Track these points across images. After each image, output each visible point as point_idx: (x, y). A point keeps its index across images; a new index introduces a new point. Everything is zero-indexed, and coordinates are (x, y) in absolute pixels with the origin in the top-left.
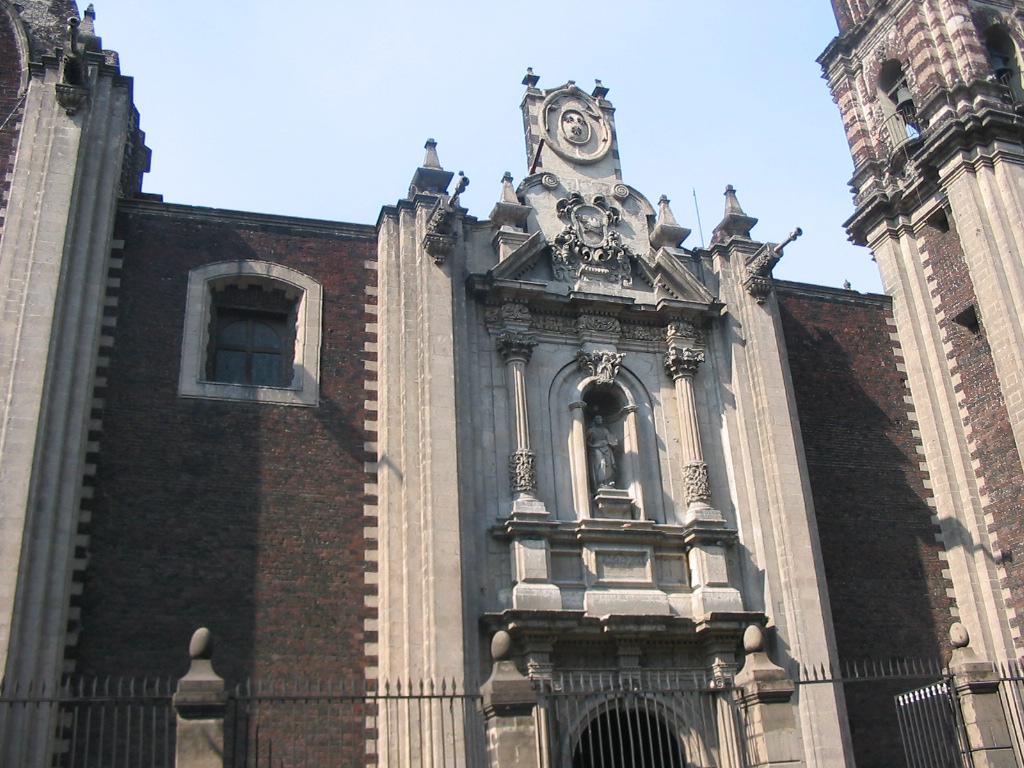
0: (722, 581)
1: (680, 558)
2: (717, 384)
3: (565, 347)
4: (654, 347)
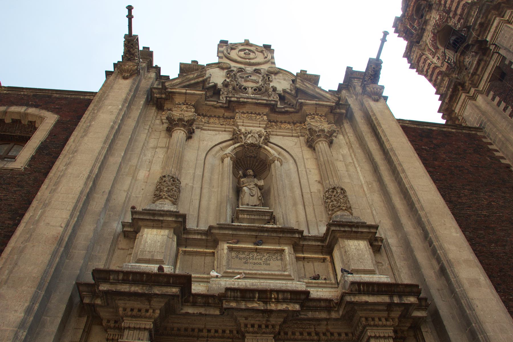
0: (367, 268)
1: (324, 260)
2: (351, 150)
4: (297, 133)
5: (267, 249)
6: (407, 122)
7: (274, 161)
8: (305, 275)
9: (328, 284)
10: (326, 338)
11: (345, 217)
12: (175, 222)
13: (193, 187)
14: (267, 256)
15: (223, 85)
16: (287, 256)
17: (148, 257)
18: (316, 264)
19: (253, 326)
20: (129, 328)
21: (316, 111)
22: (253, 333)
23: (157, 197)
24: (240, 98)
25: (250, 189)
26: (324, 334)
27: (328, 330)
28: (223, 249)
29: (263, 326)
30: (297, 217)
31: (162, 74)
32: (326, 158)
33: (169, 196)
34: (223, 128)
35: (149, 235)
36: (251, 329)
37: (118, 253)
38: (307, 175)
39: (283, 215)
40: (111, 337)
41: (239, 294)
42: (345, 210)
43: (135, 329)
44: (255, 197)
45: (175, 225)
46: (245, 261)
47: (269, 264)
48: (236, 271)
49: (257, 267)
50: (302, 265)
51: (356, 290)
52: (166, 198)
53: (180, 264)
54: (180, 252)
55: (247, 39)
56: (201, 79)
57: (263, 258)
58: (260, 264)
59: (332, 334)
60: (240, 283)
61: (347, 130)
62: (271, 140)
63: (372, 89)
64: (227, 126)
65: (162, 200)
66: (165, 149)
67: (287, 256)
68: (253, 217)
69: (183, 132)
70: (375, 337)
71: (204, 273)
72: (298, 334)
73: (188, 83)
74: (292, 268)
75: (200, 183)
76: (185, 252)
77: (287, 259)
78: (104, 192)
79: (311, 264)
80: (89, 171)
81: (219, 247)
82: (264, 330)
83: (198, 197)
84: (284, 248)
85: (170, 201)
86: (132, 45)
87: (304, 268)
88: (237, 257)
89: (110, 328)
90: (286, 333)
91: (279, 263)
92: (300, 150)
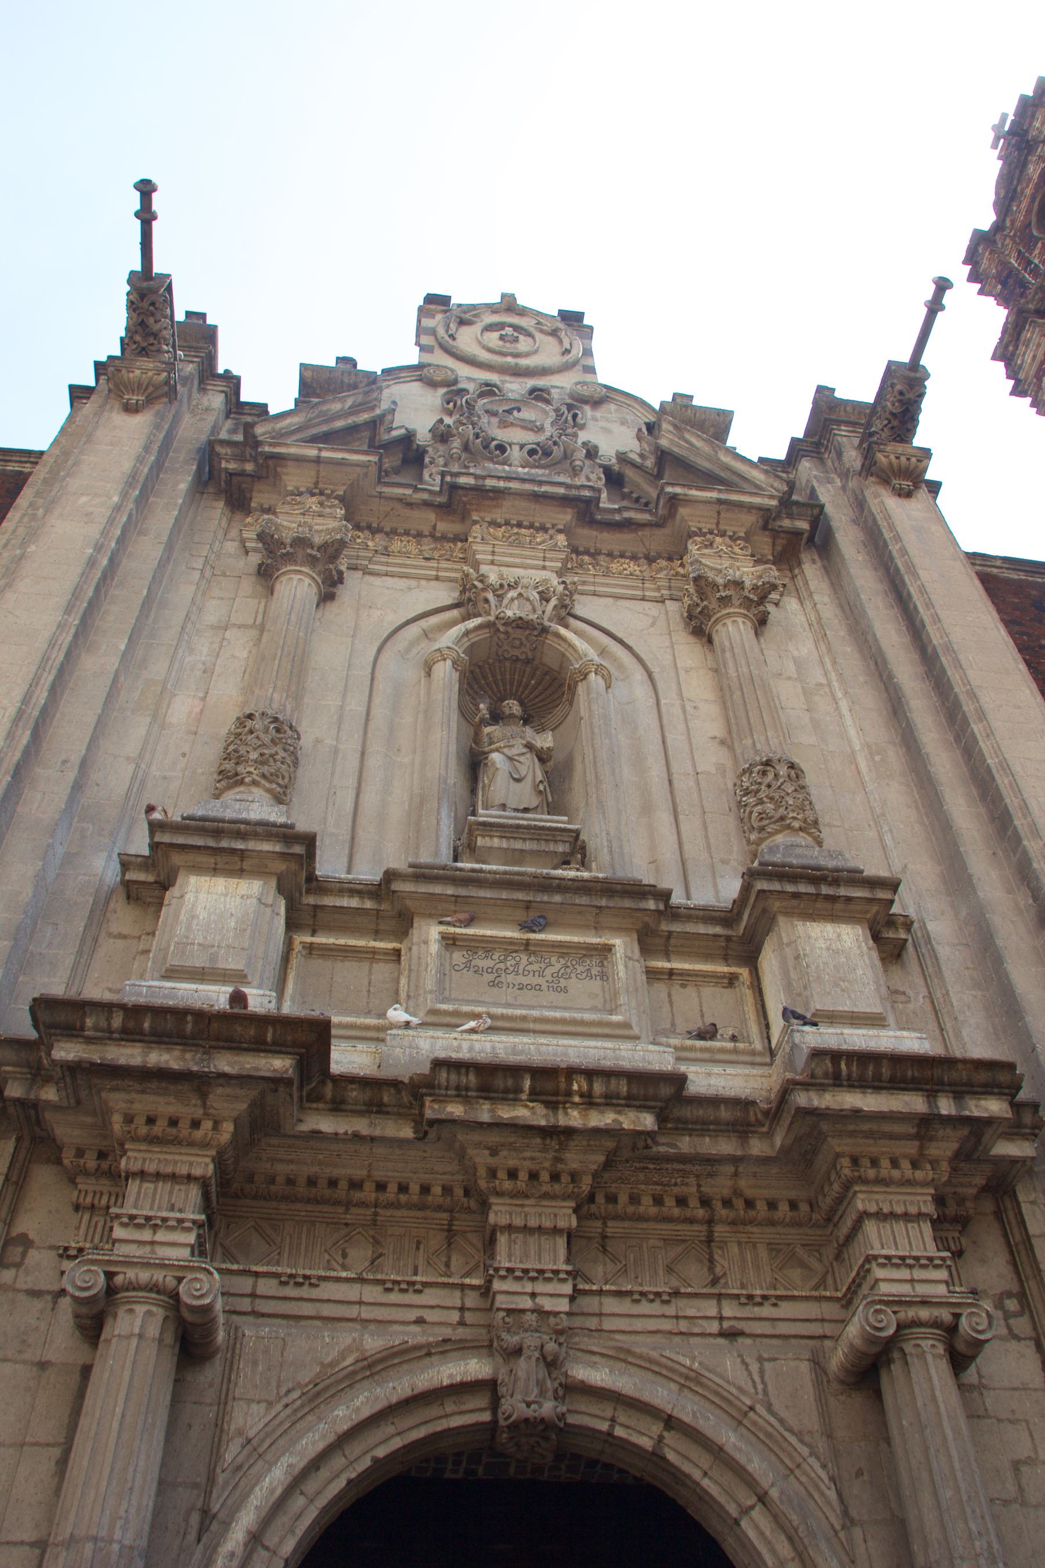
0: (862, 1007)
1: (732, 980)
2: (823, 647)
3: (433, 583)
4: (658, 589)
5: (560, 945)
6: (998, 563)
7: (585, 676)
8: (673, 1025)
9: (743, 1052)
10: (732, 1214)
11: (799, 851)
12: (283, 856)
13: (336, 751)
14: (558, 966)
15: (434, 437)
16: (621, 967)
17: (198, 963)
18: (707, 991)
19: (513, 1174)
20: (142, 1175)
21: (718, 524)
22: (515, 1195)
23: (229, 778)
24: (484, 478)
25: (511, 759)
26: (727, 1203)
27: (737, 1192)
28: (426, 942)
29: (545, 1176)
30: (653, 847)
31: (244, 397)
32: (745, 670)
33: (264, 776)
34: (431, 568)
35: (202, 896)
36: (508, 1185)
37: (108, 947)
38: (686, 719)
39: (609, 841)
40: (89, 1200)
41: (472, 1079)
42: (801, 829)
43: (158, 1176)
44: (527, 785)
45: (281, 866)
46: (491, 977)
47: (565, 990)
48: (465, 1008)
49: (528, 997)
50: (664, 995)
51: (826, 1075)
52: (254, 783)
53: (296, 983)
54: (297, 947)
55: (509, 291)
56: (365, 417)
57: (548, 972)
58: (538, 988)
59: (750, 1204)
60: (477, 1046)
61: (813, 585)
62: (579, 610)
63: (892, 457)
64: (444, 565)
65: (242, 788)
66: (254, 633)
67: (621, 967)
68: (518, 845)
69: (307, 581)
70: (881, 1216)
71: (369, 1012)
72: (647, 1200)
73: (325, 428)
74: (633, 1003)
75: (357, 737)
76: (310, 948)
77: (622, 974)
78: (65, 762)
79: (691, 991)
80: (19, 698)
81: (415, 933)
82: (546, 1188)
83: (352, 782)
84: (611, 942)
85: (268, 791)
86: (153, 304)
87: (671, 1002)
88: (468, 966)
89: (86, 1173)
90: (612, 1199)
91: (596, 985)
92: (667, 644)
